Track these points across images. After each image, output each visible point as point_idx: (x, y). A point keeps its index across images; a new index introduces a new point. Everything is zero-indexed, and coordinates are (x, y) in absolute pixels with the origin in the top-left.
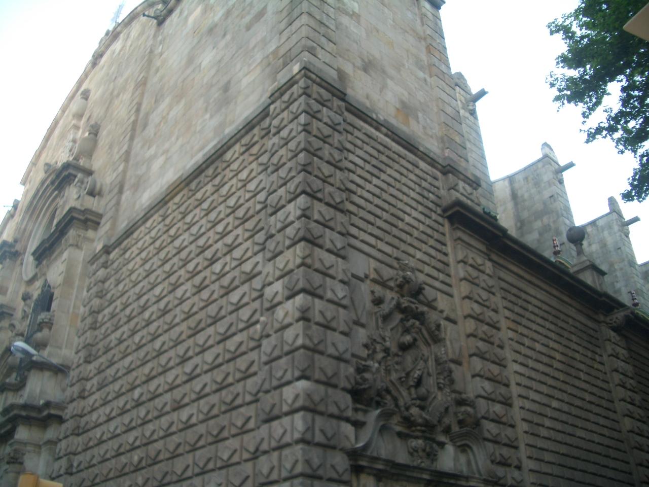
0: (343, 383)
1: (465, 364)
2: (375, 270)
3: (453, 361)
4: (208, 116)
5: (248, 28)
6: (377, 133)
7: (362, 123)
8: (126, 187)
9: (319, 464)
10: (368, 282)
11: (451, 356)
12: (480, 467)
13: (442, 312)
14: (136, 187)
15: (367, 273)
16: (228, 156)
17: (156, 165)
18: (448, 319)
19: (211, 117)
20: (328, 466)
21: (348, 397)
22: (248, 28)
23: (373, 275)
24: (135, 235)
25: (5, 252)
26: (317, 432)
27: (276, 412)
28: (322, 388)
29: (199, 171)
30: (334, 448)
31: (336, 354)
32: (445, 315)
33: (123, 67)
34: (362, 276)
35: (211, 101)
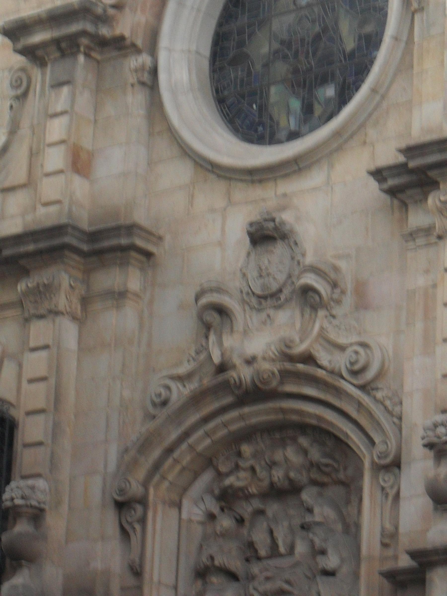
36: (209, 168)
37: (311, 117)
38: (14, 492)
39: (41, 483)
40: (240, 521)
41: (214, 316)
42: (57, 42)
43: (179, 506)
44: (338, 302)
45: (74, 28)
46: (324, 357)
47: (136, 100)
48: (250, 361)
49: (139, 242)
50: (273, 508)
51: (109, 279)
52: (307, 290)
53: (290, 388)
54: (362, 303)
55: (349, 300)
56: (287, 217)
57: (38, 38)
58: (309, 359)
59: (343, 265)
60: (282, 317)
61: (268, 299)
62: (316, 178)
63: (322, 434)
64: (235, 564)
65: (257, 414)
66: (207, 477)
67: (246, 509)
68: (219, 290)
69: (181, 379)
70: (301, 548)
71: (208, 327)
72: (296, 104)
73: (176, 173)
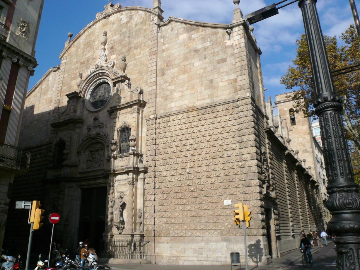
4: (203, 88)
5: (218, 62)
8: (158, 96)
14: (166, 98)
16: (219, 108)
17: (177, 95)
19: (205, 89)
22: (218, 62)
24: (172, 118)
25: (75, 96)
27: (250, 185)
29: (204, 108)
33: (134, 34)
35: (204, 83)
36: (90, 111)
37: (102, 105)
38: (65, 151)
39: (68, 150)
40: (92, 154)
41: (89, 129)
42: (72, 97)
43: (85, 153)
44: (103, 127)
45: (75, 95)
46: (101, 134)
47: (82, 103)
48: (93, 134)
49: (81, 121)
50: (96, 153)
51: (77, 125)
52: (100, 126)
53: (97, 138)
54: (106, 127)
55: (104, 127)
56: (98, 117)
57: (70, 96)
58: (99, 134)
59: (104, 123)
60: (97, 129)
61: (95, 127)
62: (102, 112)
63: (101, 143)
64: (91, 159)
65: (94, 141)
66: (89, 149)
67: (93, 153)
68: (90, 126)
69: (85, 137)
70: (99, 157)
71: (88, 131)
72: (101, 104)
73: (86, 112)
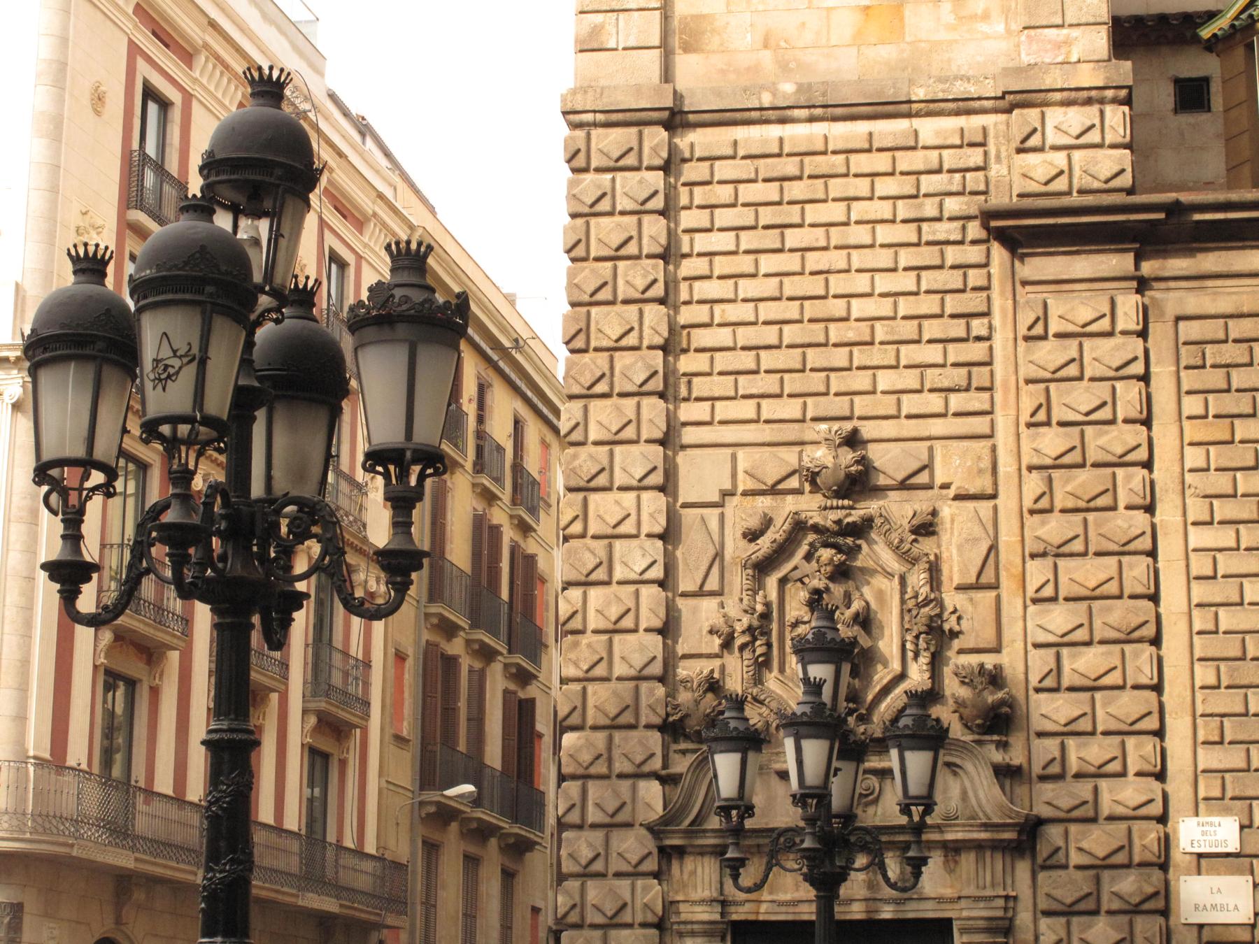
0: (646, 716)
1: (1008, 585)
2: (746, 472)
3: (961, 588)
6: (788, 130)
7: (740, 132)
9: (591, 855)
10: (736, 500)
11: (956, 581)
12: (984, 801)
13: (945, 486)
15: (727, 486)
18: (958, 498)
20: (615, 855)
21: (656, 737)
23: (744, 483)
26: (591, 808)
28: (600, 737)
30: (628, 825)
31: (632, 672)
32: (952, 492)
34: (716, 498)
